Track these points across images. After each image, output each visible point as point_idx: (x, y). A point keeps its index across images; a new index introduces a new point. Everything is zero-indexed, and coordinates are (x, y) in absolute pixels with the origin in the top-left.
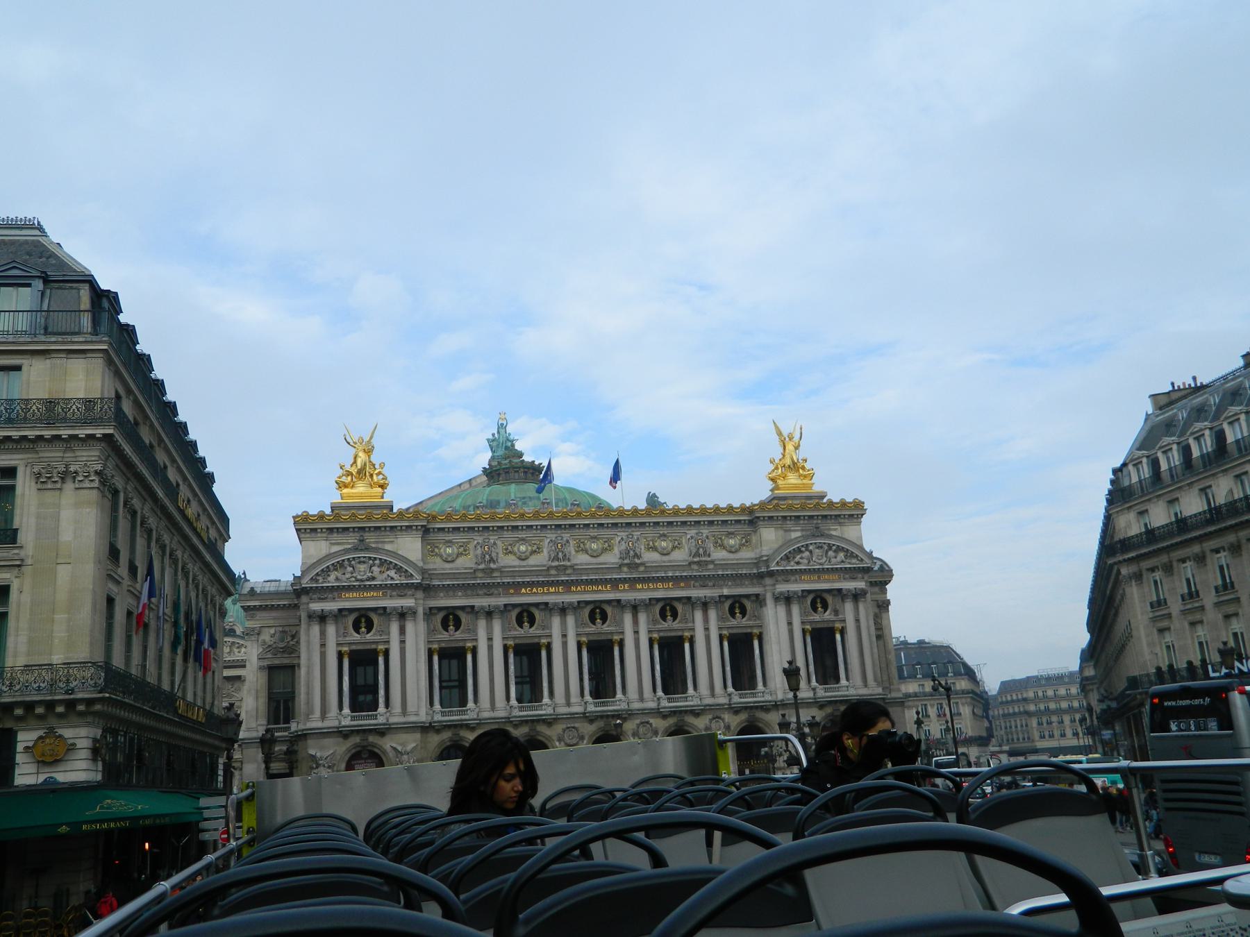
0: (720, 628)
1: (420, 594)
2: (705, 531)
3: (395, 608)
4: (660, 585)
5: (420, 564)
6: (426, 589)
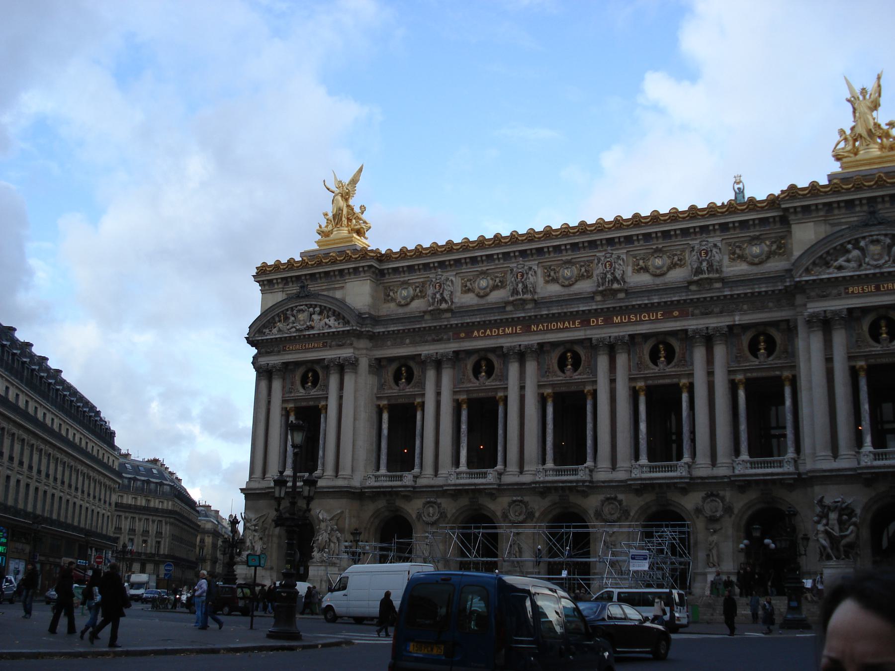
0: (730, 372)
1: (363, 344)
2: (716, 239)
3: (331, 360)
4: (645, 317)
5: (365, 309)
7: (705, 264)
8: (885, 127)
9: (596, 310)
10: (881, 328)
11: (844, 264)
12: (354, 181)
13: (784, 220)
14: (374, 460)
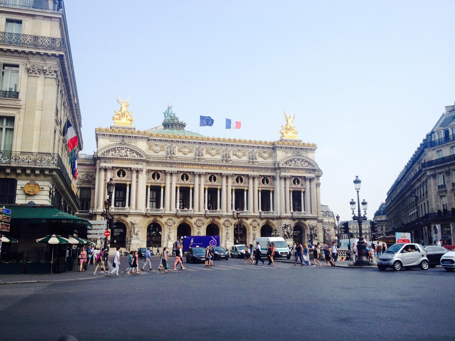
1: (144, 164)
2: (256, 150)
5: (146, 152)
6: (148, 162)
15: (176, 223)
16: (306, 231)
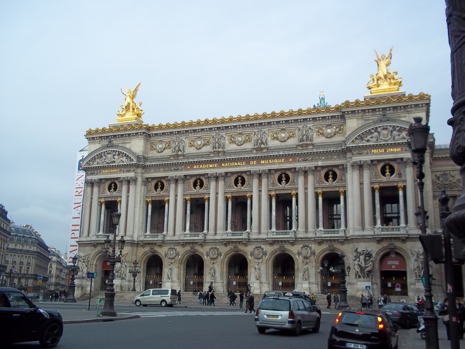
0: (315, 188)
1: (139, 170)
2: (310, 125)
4: (276, 161)
5: (141, 154)
6: (144, 167)
7: (305, 137)
8: (392, 74)
9: (253, 157)
10: (386, 169)
11: (370, 139)
12: (136, 90)
13: (343, 117)
14: (144, 227)
15: (180, 255)
16: (407, 263)
